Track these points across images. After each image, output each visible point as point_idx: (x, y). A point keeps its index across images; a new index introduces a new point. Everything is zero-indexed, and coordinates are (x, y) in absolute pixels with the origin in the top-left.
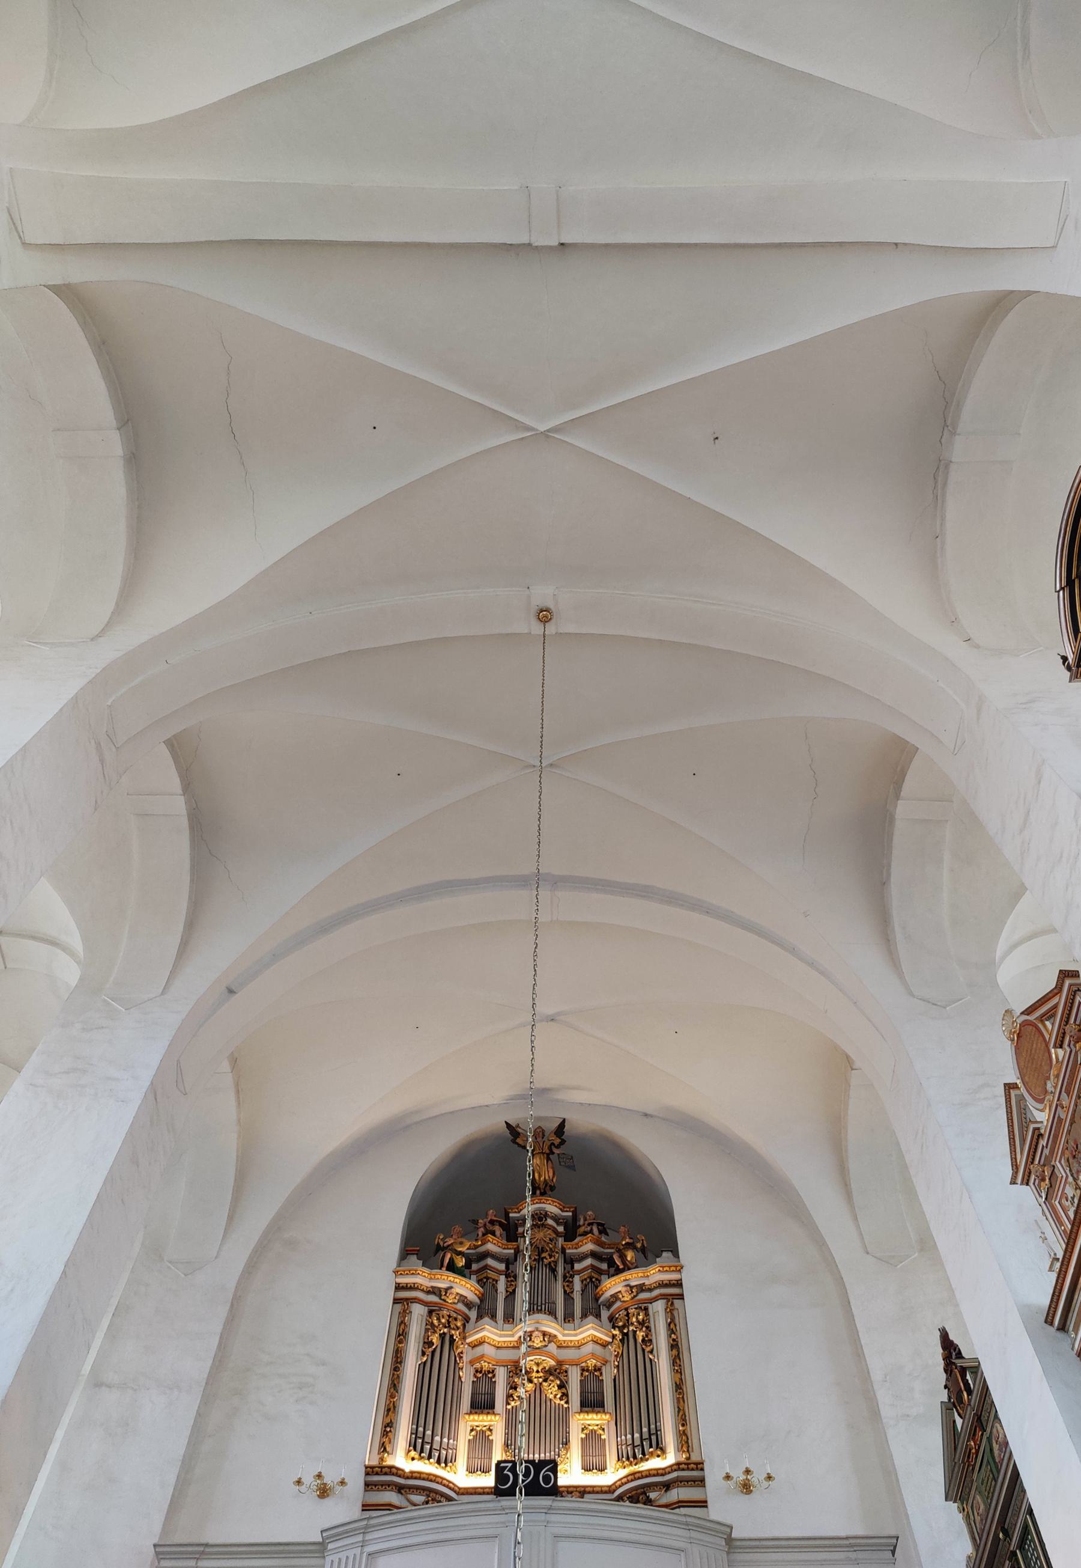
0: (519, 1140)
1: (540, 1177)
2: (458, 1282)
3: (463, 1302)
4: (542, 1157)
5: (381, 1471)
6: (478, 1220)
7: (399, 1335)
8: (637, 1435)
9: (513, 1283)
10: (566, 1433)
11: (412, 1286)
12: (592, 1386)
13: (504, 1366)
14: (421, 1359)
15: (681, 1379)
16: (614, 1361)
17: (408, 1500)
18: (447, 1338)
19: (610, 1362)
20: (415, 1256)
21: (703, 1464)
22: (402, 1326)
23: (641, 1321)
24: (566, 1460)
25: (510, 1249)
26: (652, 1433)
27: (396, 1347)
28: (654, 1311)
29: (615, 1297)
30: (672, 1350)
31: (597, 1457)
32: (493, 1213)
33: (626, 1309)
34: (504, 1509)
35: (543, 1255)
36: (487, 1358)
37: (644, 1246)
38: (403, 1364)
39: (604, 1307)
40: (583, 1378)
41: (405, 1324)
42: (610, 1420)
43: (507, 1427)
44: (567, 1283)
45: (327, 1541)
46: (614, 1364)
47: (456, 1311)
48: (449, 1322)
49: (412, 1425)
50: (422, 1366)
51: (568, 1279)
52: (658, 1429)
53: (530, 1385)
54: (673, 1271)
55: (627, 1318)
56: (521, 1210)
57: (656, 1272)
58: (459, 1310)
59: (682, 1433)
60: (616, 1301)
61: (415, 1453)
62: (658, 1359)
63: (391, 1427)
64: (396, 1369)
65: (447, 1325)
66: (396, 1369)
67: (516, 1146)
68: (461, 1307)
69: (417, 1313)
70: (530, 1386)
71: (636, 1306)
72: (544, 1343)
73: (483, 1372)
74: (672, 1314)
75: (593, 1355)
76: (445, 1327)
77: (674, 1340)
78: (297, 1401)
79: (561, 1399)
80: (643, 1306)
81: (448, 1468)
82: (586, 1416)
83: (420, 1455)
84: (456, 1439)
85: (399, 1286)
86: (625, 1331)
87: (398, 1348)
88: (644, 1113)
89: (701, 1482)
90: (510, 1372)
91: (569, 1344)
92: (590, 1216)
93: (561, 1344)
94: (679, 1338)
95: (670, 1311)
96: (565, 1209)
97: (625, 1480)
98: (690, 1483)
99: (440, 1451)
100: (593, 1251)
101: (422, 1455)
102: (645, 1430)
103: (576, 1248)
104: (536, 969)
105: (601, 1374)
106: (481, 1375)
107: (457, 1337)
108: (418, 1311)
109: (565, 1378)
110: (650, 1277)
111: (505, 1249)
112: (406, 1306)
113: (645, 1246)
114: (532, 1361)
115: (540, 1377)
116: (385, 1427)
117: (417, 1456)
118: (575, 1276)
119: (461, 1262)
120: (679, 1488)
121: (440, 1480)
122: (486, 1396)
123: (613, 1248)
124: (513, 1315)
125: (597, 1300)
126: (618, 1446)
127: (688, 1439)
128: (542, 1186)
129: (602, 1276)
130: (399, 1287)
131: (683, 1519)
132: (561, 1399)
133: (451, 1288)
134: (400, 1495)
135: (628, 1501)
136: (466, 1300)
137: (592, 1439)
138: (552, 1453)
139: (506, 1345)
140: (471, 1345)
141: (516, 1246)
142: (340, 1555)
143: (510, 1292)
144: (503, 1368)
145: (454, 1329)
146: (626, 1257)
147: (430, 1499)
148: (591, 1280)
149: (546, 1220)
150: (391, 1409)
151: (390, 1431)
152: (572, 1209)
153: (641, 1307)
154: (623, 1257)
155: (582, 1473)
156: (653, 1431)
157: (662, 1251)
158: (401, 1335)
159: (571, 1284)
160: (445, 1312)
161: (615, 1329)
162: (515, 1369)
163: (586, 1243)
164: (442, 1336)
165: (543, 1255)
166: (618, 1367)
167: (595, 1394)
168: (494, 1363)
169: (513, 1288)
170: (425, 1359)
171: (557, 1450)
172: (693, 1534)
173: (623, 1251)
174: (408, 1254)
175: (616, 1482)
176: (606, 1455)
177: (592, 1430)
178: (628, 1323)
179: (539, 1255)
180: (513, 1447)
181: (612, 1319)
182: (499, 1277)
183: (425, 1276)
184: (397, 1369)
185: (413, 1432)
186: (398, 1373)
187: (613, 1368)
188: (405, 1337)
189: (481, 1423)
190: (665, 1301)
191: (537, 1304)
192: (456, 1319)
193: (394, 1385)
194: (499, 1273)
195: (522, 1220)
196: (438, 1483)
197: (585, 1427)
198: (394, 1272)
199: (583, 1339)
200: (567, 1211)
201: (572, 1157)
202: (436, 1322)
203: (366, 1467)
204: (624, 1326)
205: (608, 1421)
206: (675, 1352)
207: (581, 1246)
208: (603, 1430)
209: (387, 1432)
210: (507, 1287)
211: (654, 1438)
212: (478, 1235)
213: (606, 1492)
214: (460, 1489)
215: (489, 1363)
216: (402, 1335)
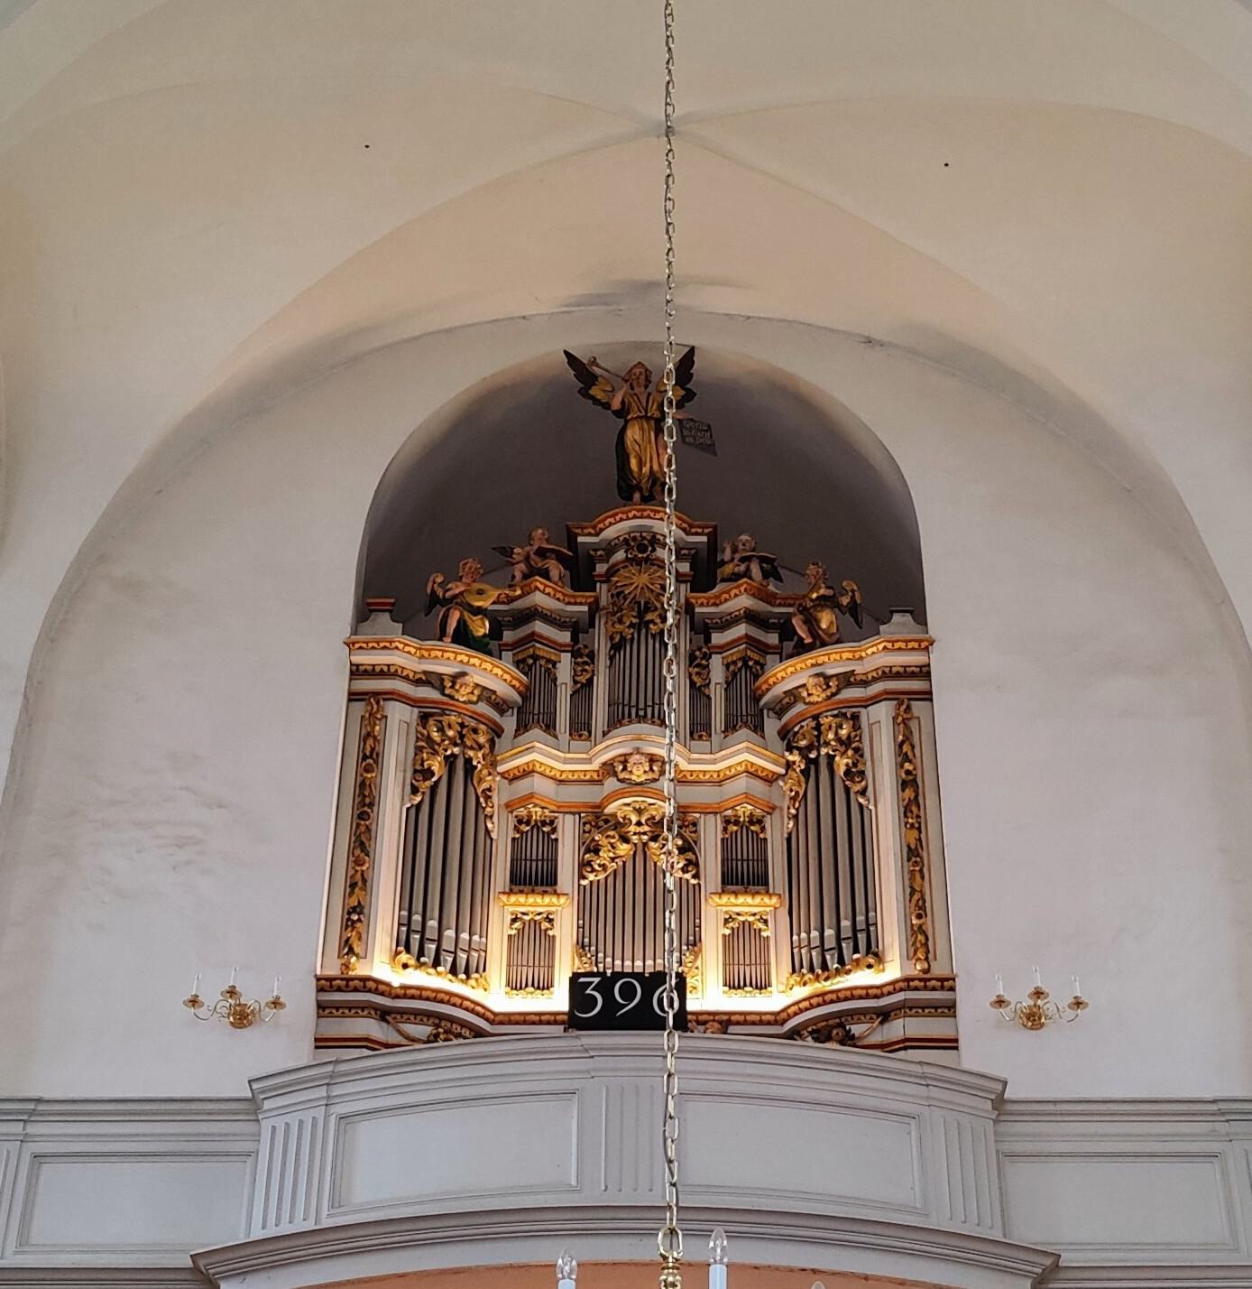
0: (594, 391)
1: (641, 464)
2: (477, 664)
3: (488, 701)
4: (645, 425)
5: (347, 986)
6: (512, 549)
7: (365, 757)
8: (829, 932)
10: (695, 927)
11: (385, 669)
12: (744, 849)
13: (573, 813)
14: (411, 800)
15: (920, 840)
16: (789, 808)
17: (400, 1032)
18: (460, 763)
19: (781, 809)
20: (387, 614)
21: (954, 980)
22: (370, 742)
23: (844, 738)
24: (694, 970)
25: (581, 604)
27: (359, 779)
28: (872, 721)
29: (794, 696)
30: (903, 791)
31: (753, 967)
32: (543, 534)
33: (816, 717)
34: (586, 1051)
35: (649, 617)
36: (538, 799)
37: (855, 601)
38: (375, 809)
39: (771, 713)
40: (727, 836)
41: (375, 738)
42: (778, 906)
43: (581, 916)
44: (696, 669)
45: (262, 1097)
46: (789, 813)
47: (477, 717)
48: (462, 736)
49: (399, 912)
50: (413, 811)
52: (870, 922)
53: (625, 846)
54: (913, 649)
56: (602, 530)
57: (878, 651)
58: (482, 716)
59: (915, 929)
60: (795, 702)
61: (408, 956)
62: (876, 806)
63: (359, 914)
64: (363, 816)
65: (459, 741)
66: (363, 816)
67: (591, 402)
68: (483, 708)
69: (397, 717)
70: (624, 849)
71: (836, 712)
72: (651, 776)
73: (533, 823)
74: (907, 727)
75: (748, 798)
76: (456, 745)
77: (908, 773)
78: (174, 868)
79: (684, 870)
80: (849, 712)
81: (472, 982)
82: (733, 899)
83: (418, 960)
84: (484, 933)
85: (357, 670)
86: (812, 756)
87: (364, 780)
88: (868, 337)
89: (949, 1009)
90: (585, 824)
91: (701, 776)
92: (744, 545)
93: (685, 776)
95: (904, 722)
96: (693, 530)
97: (806, 1004)
98: (927, 1011)
99: (455, 953)
100: (750, 611)
101: (422, 959)
102: (846, 923)
103: (715, 605)
104: (672, 46)
105: (763, 829)
106: (528, 828)
107: (479, 762)
108: (399, 717)
109: (693, 835)
110: (865, 660)
111: (569, 603)
112: (375, 706)
113: (858, 602)
114: (628, 805)
115: (645, 833)
116: (349, 913)
117: (412, 962)
118: (713, 656)
119: (481, 628)
120: (906, 1019)
121: (458, 1001)
122: (540, 863)
123: (790, 605)
124: (590, 725)
125: (757, 699)
126: (792, 948)
127: (927, 939)
128: (645, 484)
129: (768, 656)
130: (357, 672)
131: (918, 1069)
132: (684, 870)
133: (464, 674)
134: (384, 1024)
135: (809, 1039)
136: (493, 697)
137: (742, 937)
139: (576, 777)
140: (506, 776)
141: (592, 599)
142: (288, 1119)
143: (582, 684)
144: (571, 816)
145: (471, 748)
146: (818, 621)
147: (441, 1030)
148: (745, 665)
149: (654, 550)
150: (358, 884)
151: (359, 920)
152: (706, 531)
153: (845, 714)
154: (811, 623)
155: (724, 992)
156: (861, 924)
157: (892, 612)
158: (369, 757)
159: (705, 672)
160: (453, 718)
161: (791, 753)
162: (597, 820)
163: (736, 595)
164: (450, 761)
165: (649, 617)
166: (796, 817)
167: (751, 863)
168: (555, 808)
169: (588, 676)
170: (418, 799)
172: (935, 1092)
174: (371, 611)
175: (789, 1007)
176: (769, 964)
177: (744, 922)
178: (818, 741)
179: (640, 615)
180: (593, 948)
181: (784, 733)
183: (409, 653)
184: (366, 817)
185: (401, 922)
186: (367, 823)
187: (786, 818)
188: (376, 762)
189: (532, 909)
190: (895, 702)
192: (475, 731)
193: (361, 843)
194: (560, 648)
195: (603, 550)
196: (454, 1005)
197: (730, 917)
198: (345, 643)
199: (729, 768)
200: (697, 534)
201: (709, 426)
202: (436, 736)
203: (318, 979)
204: (810, 748)
205: (776, 908)
206: (909, 793)
207: (726, 600)
208: (766, 922)
209: (354, 922)
210: (576, 675)
211: (862, 937)
212: (514, 577)
213: (769, 1023)
214: (495, 1014)
215: (543, 808)
216: (371, 757)
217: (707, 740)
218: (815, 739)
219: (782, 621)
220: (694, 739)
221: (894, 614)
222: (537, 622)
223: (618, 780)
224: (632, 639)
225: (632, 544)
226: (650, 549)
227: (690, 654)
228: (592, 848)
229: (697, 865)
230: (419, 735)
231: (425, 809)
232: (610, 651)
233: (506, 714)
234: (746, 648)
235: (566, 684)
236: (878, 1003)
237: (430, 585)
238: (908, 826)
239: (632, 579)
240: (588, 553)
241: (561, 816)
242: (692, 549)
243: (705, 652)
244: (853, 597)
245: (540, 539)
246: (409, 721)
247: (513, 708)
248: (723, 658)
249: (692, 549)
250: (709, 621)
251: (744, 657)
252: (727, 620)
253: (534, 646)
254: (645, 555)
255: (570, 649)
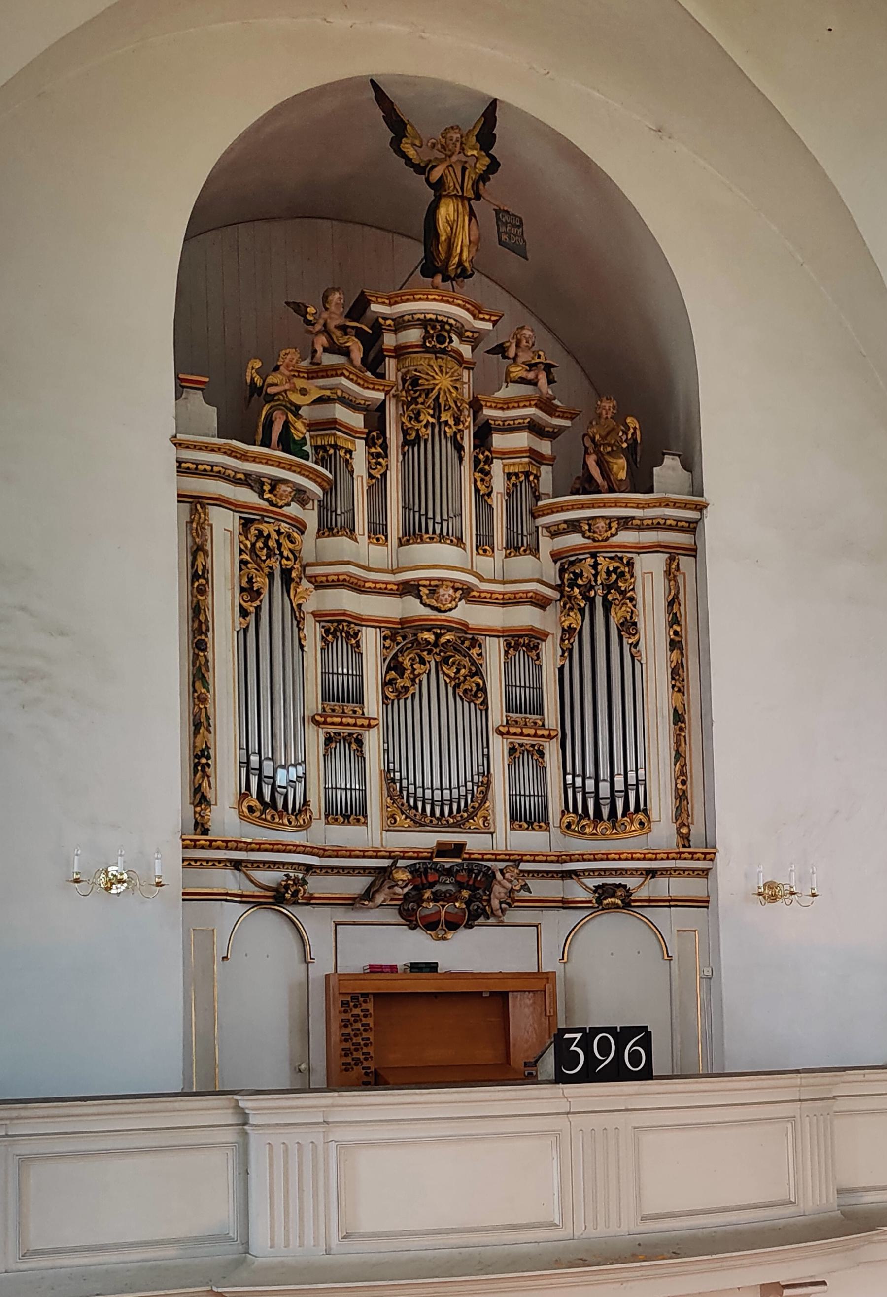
6: (306, 307)
9: (381, 460)
17: (249, 877)
20: (200, 392)
25: (378, 390)
26: (630, 782)
30: (672, 651)
33: (594, 555)
37: (636, 440)
38: (210, 634)
39: (544, 530)
44: (480, 474)
50: (242, 633)
51: (482, 468)
55: (593, 572)
56: (396, 303)
74: (676, 581)
77: (676, 633)
92: (527, 342)
94: (683, 631)
95: (671, 574)
96: (481, 316)
102: (619, 781)
103: (502, 409)
111: (368, 388)
112: (202, 516)
113: (639, 441)
118: (495, 460)
123: (567, 418)
129: (543, 468)
138: (463, 790)
140: (313, 580)
144: (373, 629)
145: (288, 559)
149: (451, 341)
152: (493, 318)
156: (632, 780)
159: (487, 478)
169: (382, 472)
171: (469, 784)
173: (606, 457)
178: (596, 581)
180: (397, 774)
182: (354, 443)
185: (242, 761)
186: (206, 653)
191: (434, 518)
195: (393, 320)
198: (172, 441)
200: (484, 319)
210: (370, 468)
212: (315, 351)
217: (490, 556)
218: (593, 579)
219: (556, 430)
220: (478, 553)
221: (666, 456)
222: (337, 405)
223: (421, 603)
224: (426, 441)
225: (432, 332)
226: (448, 341)
227: (475, 457)
228: (392, 665)
229: (484, 690)
230: (242, 547)
231: (252, 630)
232: (403, 446)
233: (307, 507)
234: (530, 463)
235: (362, 477)
236: (651, 864)
237: (249, 371)
238: (676, 689)
239: (434, 379)
240: (377, 319)
241: (364, 628)
242: (476, 332)
243: (487, 456)
244: (634, 434)
245: (337, 304)
246: (231, 529)
247: (313, 501)
248: (504, 465)
249: (476, 332)
250: (492, 422)
251: (527, 472)
252: (509, 424)
253: (334, 435)
254: (443, 346)
255: (364, 436)
